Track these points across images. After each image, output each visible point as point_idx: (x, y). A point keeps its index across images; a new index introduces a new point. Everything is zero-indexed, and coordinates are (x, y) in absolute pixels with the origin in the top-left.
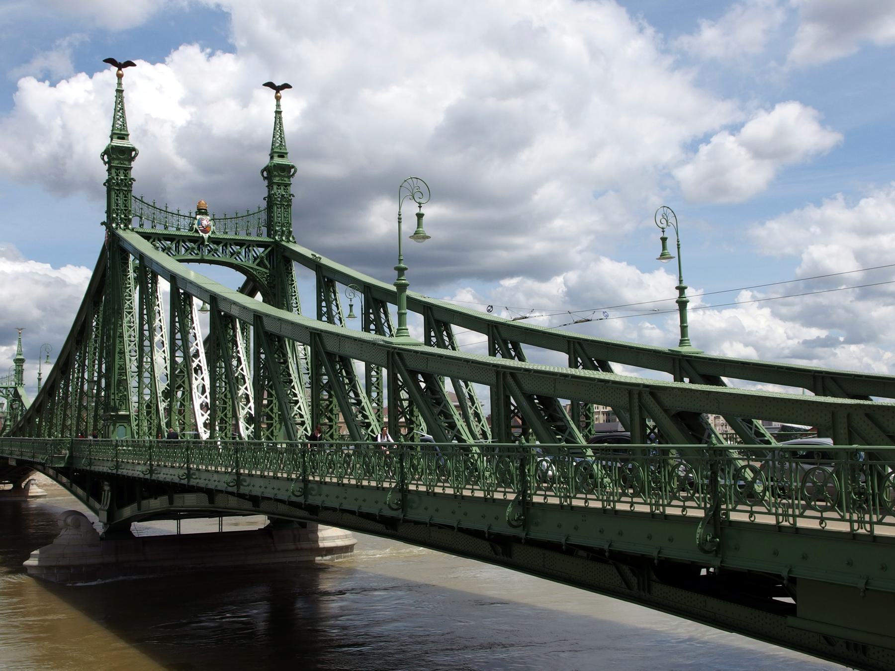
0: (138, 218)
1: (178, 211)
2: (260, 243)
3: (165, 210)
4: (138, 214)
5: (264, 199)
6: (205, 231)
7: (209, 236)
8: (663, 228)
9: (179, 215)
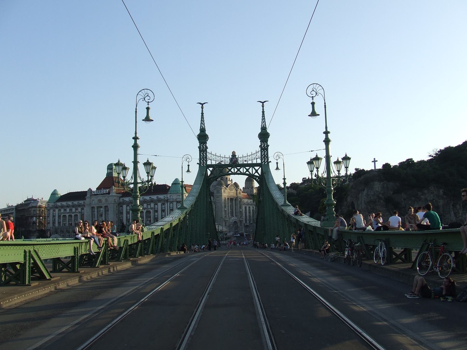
0: (210, 160)
5: (260, 147)
7: (235, 165)
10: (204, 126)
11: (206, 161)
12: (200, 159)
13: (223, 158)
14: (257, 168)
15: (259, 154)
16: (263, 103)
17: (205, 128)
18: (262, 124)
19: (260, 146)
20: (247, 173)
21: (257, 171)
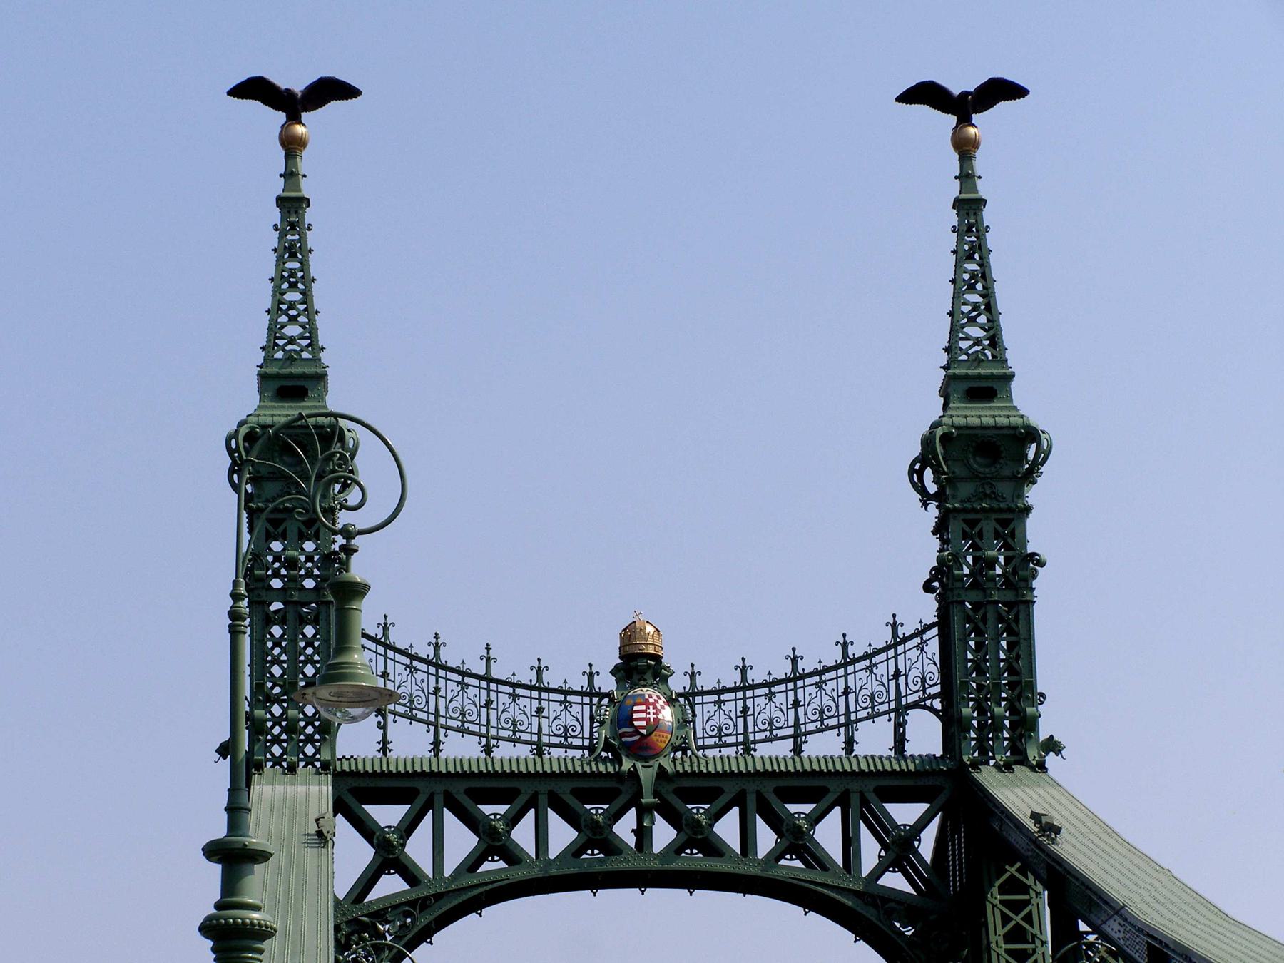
1: (539, 671)
3: (482, 672)
5: (928, 587)
10: (311, 332)
12: (261, 697)
13: (514, 697)
14: (905, 813)
17: (316, 360)
18: (955, 330)
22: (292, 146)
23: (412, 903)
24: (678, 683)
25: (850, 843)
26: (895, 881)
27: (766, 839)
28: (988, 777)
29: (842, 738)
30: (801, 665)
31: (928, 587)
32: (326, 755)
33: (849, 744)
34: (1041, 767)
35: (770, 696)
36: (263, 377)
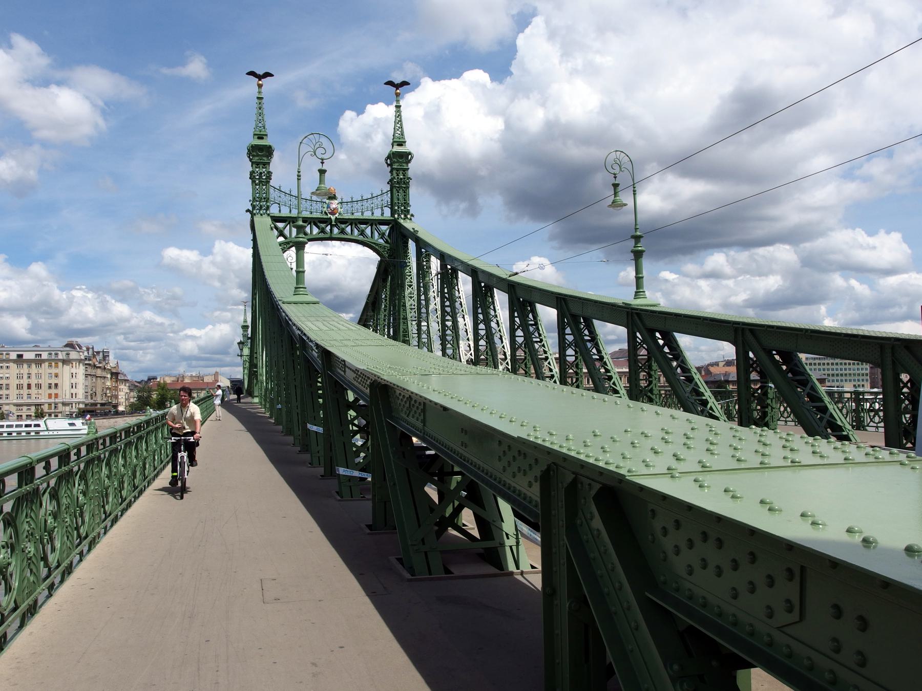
2: (381, 221)
4: (277, 202)
6: (333, 213)
7: (336, 218)
8: (615, 174)
9: (311, 201)
11: (268, 208)
14: (384, 228)
15: (387, 198)
16: (397, 86)
19: (391, 182)
20: (361, 238)
21: (382, 235)
22: (260, 86)
23: (286, 243)
24: (340, 201)
25: (372, 233)
26: (381, 241)
27: (356, 232)
28: (402, 221)
29: (371, 213)
30: (363, 197)
31: (388, 183)
32: (268, 212)
33: (373, 214)
34: (411, 219)
35: (357, 204)
36: (255, 135)
